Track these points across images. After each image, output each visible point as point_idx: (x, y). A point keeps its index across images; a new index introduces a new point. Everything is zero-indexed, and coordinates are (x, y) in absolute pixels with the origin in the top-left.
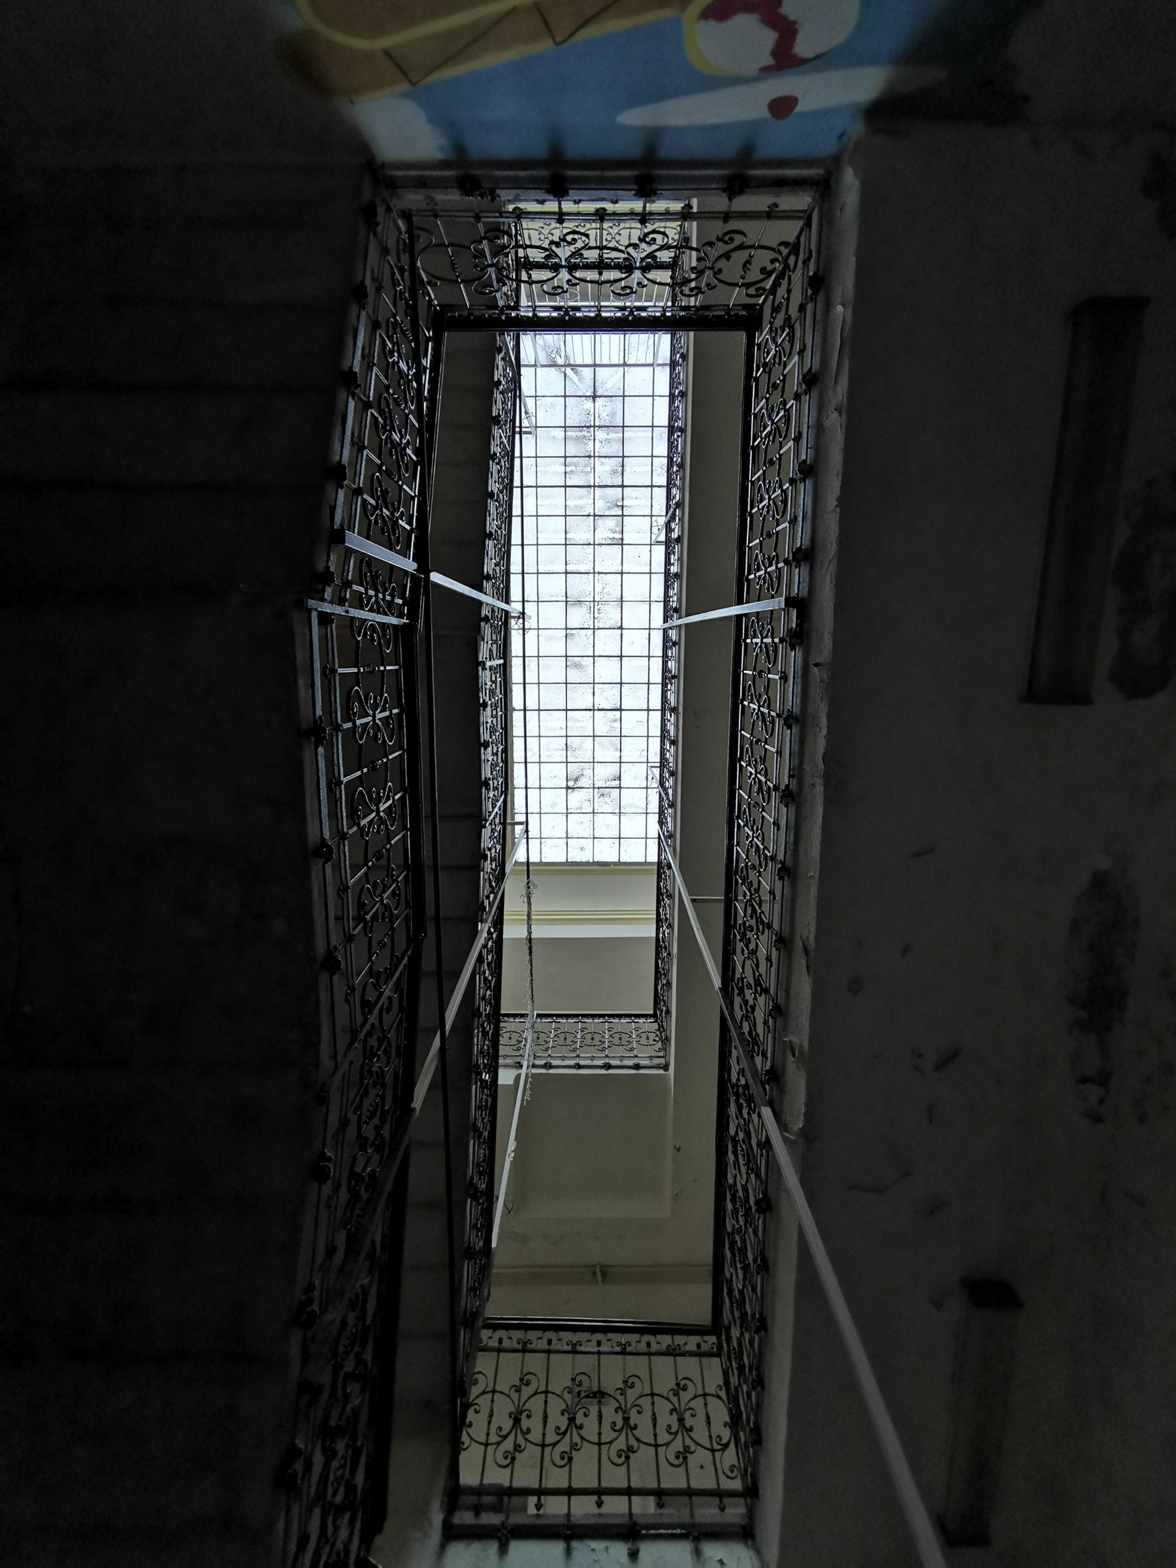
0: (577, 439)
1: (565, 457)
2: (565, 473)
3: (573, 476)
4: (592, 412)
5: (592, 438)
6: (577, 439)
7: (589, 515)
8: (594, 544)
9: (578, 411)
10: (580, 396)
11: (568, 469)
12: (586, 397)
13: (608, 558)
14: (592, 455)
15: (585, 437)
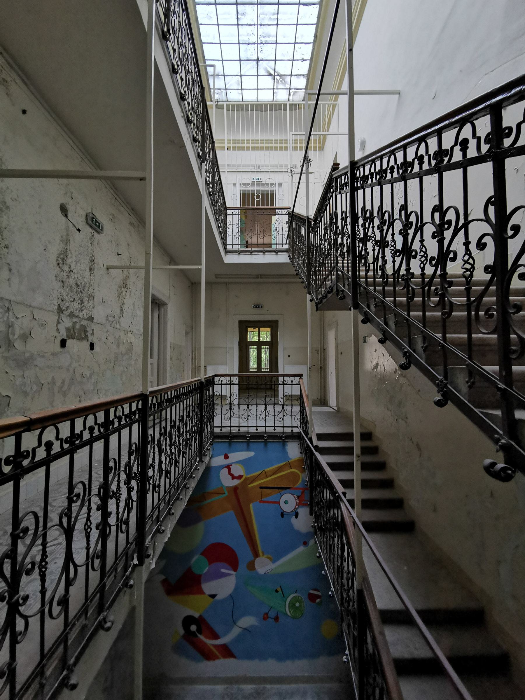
0: (269, 36)
1: (277, 25)
2: (278, 14)
3: (273, 11)
5: (259, 37)
6: (269, 36)
9: (267, 52)
10: (267, 60)
11: (276, 16)
14: (259, 26)
15: (264, 37)
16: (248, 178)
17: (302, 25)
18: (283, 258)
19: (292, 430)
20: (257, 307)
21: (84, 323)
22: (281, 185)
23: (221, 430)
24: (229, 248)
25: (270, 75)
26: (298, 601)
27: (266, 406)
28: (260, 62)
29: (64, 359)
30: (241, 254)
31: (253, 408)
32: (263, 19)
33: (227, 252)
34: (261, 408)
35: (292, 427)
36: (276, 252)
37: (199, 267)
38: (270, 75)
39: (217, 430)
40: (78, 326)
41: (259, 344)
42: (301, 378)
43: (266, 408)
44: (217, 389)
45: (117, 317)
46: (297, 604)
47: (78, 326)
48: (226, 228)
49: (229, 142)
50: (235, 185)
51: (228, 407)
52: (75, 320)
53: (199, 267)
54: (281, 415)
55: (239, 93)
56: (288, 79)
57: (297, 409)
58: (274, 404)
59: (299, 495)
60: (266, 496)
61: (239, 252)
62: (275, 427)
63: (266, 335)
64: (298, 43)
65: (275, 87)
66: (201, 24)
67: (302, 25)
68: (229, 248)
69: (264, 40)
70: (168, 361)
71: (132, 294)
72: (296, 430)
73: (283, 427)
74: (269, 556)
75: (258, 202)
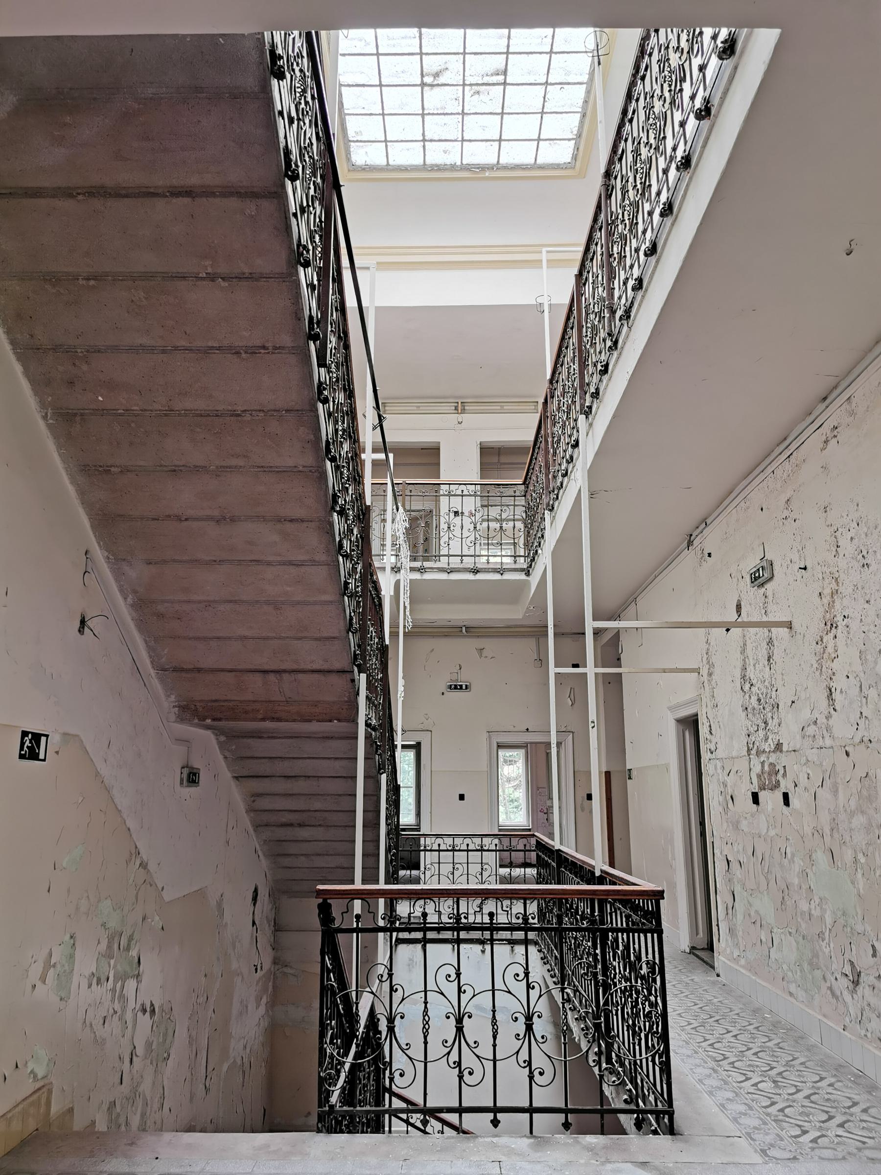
21: (773, 758)
40: (766, 768)
47: (766, 768)
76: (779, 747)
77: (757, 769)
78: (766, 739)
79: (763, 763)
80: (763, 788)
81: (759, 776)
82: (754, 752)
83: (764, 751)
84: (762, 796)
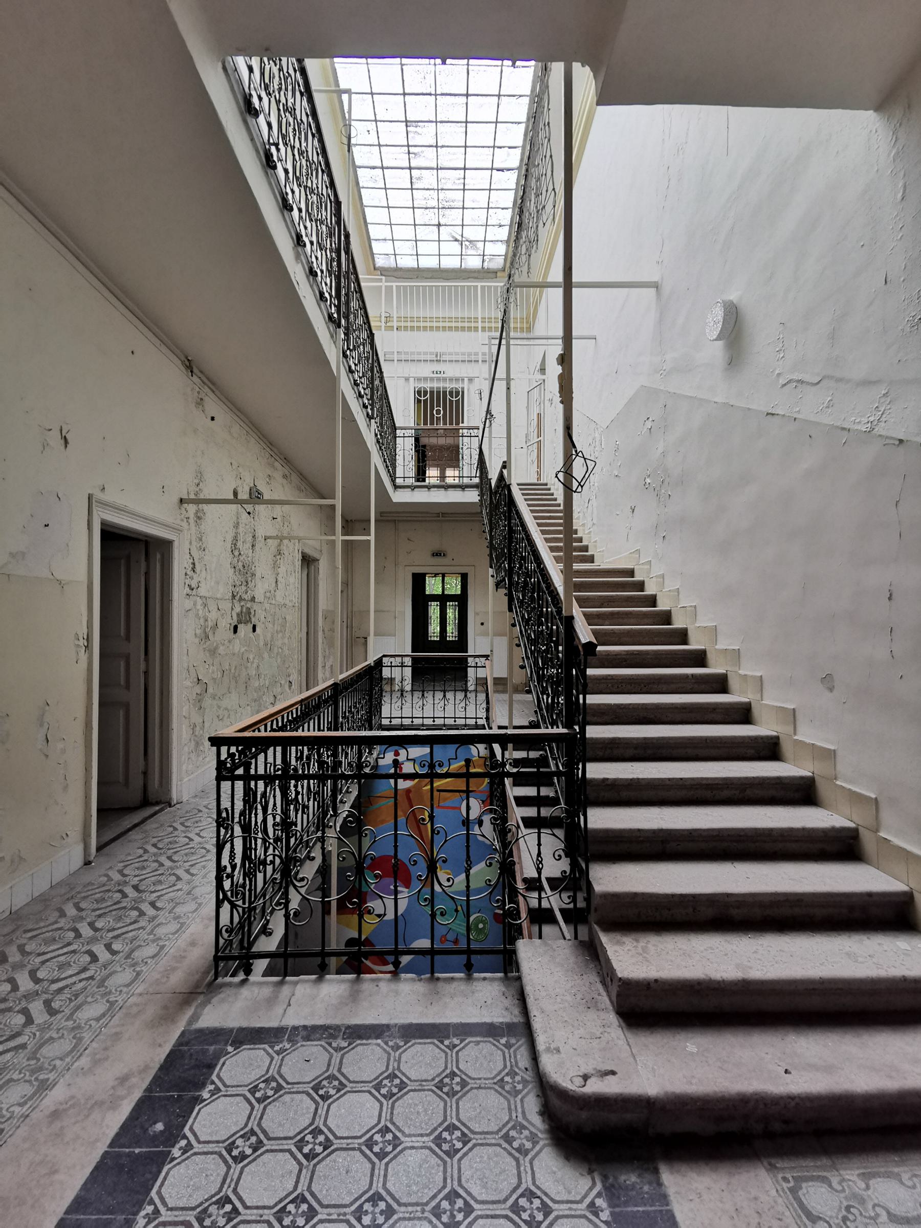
2: (464, 178)
3: (458, 176)
4: (440, 217)
7: (443, 146)
8: (436, 122)
9: (454, 216)
12: (446, 225)
13: (420, 109)
16: (425, 370)
17: (497, 190)
18: (472, 496)
19: (476, 722)
20: (437, 554)
21: (249, 605)
22: (471, 380)
23: (391, 722)
24: (399, 481)
25: (456, 240)
26: (482, 922)
27: (445, 693)
28: (441, 228)
29: (237, 646)
30: (416, 490)
31: (429, 695)
32: (445, 184)
33: (396, 487)
34: (439, 695)
35: (476, 718)
36: (463, 487)
37: (368, 538)
38: (456, 240)
39: (385, 722)
40: (244, 610)
41: (443, 599)
42: (487, 659)
43: (445, 696)
44: (386, 673)
45: (273, 592)
46: (481, 926)
47: (244, 610)
48: (396, 455)
49: (399, 319)
50: (407, 379)
51: (399, 694)
52: (242, 604)
53: (368, 538)
54: (463, 704)
55: (413, 259)
56: (480, 245)
57: (481, 697)
58: (455, 691)
59: (484, 799)
60: (445, 799)
61: (413, 488)
62: (455, 718)
63: (453, 586)
64: (492, 208)
65: (463, 253)
66: (363, 188)
67: (497, 190)
68: (399, 481)
69: (446, 205)
70: (320, 634)
71: (286, 559)
72: (480, 722)
73: (466, 718)
74: (449, 871)
75: (438, 419)
76: (253, 599)
77: (238, 609)
78: (246, 593)
79: (242, 607)
80: (240, 622)
81: (238, 615)
82: (237, 598)
83: (244, 600)
84: (241, 627)
